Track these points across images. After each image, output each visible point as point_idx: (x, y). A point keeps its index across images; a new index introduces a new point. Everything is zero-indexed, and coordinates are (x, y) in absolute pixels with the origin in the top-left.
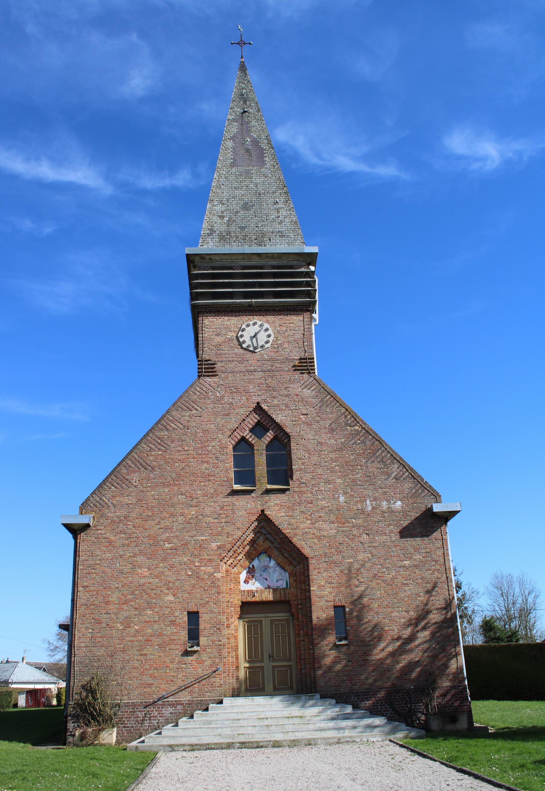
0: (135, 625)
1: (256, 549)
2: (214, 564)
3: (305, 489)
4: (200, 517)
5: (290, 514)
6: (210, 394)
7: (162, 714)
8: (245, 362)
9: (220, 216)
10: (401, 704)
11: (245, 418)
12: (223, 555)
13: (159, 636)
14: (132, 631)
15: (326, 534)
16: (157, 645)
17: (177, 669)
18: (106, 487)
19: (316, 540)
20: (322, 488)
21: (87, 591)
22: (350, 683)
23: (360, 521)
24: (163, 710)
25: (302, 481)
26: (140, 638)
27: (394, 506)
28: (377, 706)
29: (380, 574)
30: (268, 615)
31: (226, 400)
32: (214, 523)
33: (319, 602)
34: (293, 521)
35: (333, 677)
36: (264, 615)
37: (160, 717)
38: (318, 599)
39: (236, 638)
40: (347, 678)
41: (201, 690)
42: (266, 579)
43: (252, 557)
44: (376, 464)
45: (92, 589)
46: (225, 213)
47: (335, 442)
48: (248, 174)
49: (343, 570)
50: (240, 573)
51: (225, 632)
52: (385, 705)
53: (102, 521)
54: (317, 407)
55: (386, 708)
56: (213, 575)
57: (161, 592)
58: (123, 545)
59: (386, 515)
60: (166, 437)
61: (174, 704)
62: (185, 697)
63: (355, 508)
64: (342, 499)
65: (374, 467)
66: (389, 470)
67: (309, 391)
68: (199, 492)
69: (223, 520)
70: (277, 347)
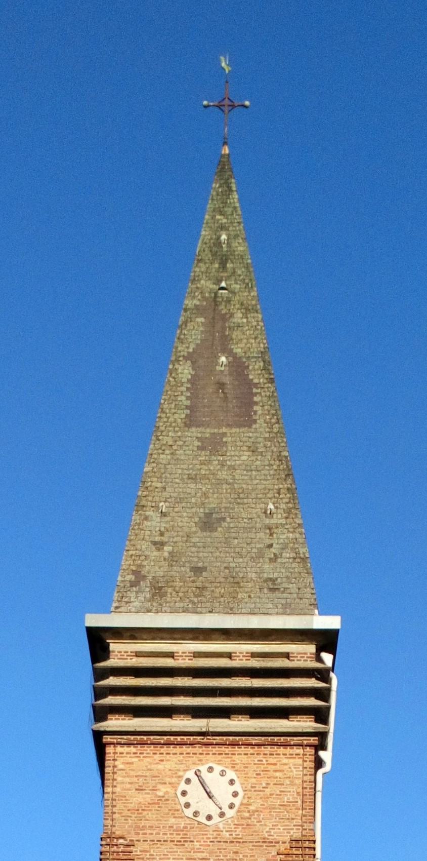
8: (186, 844)
9: (155, 543)
46: (167, 534)
48: (213, 445)
70: (246, 816)
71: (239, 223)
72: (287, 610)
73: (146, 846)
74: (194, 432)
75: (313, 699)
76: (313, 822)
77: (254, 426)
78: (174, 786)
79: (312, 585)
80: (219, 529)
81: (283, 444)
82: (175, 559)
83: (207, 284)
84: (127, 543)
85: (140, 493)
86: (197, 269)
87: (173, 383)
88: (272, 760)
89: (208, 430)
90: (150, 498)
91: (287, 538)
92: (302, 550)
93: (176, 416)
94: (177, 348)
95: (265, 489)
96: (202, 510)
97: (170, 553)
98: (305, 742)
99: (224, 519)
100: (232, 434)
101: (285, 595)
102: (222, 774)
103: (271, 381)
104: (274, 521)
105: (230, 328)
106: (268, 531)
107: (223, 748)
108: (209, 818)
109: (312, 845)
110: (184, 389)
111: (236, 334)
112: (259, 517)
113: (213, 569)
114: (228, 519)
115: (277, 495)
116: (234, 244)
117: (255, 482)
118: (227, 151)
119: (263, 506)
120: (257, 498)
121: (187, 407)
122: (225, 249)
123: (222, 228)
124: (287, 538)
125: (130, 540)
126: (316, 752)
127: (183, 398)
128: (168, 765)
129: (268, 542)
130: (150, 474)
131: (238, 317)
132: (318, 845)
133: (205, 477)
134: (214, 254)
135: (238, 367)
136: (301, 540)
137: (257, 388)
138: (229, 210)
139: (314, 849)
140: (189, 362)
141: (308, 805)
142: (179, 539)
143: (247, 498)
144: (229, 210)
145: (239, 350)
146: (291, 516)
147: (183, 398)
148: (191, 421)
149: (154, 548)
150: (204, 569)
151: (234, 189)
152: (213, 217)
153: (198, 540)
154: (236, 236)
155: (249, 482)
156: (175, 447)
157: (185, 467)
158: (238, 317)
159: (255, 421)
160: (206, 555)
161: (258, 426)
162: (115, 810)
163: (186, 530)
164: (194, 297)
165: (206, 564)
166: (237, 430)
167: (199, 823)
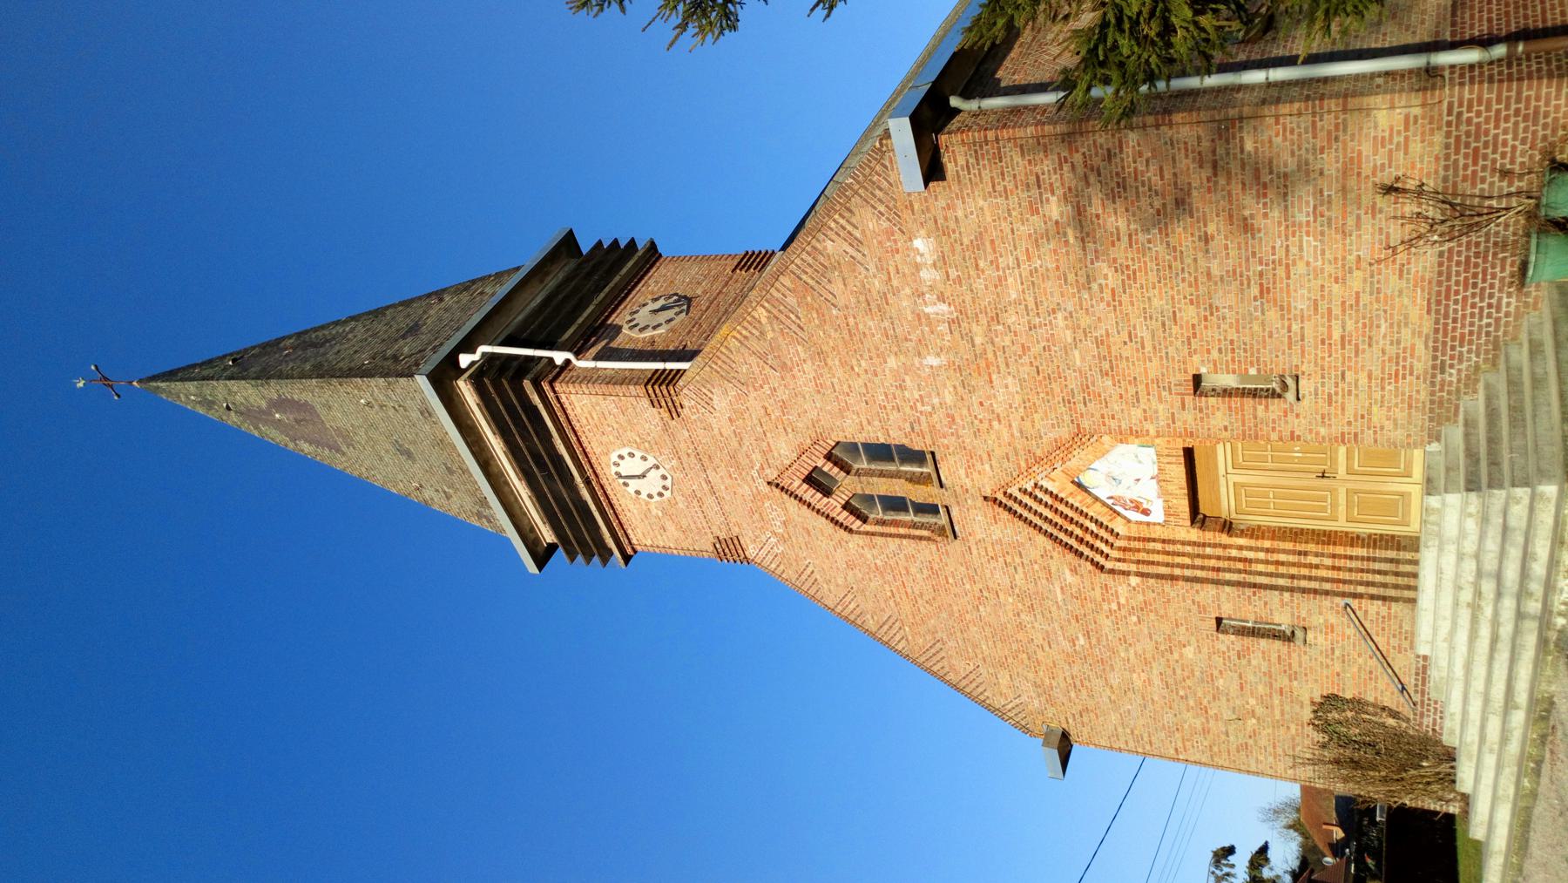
4: (1017, 591)
15: (1018, 399)
20: (917, 397)
25: (908, 429)
26: (1277, 702)
27: (927, 256)
28: (1480, 327)
29: (1107, 295)
30: (1222, 471)
33: (1185, 422)
34: (998, 452)
36: (1222, 481)
38: (1178, 424)
40: (1390, 383)
42: (1138, 480)
44: (837, 287)
47: (809, 362)
49: (1101, 371)
54: (744, 388)
55: (1490, 306)
56: (1134, 589)
60: (875, 618)
63: (948, 337)
64: (932, 360)
66: (842, 262)
67: (715, 397)
68: (968, 586)
69: (1018, 560)
88: (584, 421)
107: (593, 461)
108: (664, 478)
128: (631, 507)
162: (691, 548)
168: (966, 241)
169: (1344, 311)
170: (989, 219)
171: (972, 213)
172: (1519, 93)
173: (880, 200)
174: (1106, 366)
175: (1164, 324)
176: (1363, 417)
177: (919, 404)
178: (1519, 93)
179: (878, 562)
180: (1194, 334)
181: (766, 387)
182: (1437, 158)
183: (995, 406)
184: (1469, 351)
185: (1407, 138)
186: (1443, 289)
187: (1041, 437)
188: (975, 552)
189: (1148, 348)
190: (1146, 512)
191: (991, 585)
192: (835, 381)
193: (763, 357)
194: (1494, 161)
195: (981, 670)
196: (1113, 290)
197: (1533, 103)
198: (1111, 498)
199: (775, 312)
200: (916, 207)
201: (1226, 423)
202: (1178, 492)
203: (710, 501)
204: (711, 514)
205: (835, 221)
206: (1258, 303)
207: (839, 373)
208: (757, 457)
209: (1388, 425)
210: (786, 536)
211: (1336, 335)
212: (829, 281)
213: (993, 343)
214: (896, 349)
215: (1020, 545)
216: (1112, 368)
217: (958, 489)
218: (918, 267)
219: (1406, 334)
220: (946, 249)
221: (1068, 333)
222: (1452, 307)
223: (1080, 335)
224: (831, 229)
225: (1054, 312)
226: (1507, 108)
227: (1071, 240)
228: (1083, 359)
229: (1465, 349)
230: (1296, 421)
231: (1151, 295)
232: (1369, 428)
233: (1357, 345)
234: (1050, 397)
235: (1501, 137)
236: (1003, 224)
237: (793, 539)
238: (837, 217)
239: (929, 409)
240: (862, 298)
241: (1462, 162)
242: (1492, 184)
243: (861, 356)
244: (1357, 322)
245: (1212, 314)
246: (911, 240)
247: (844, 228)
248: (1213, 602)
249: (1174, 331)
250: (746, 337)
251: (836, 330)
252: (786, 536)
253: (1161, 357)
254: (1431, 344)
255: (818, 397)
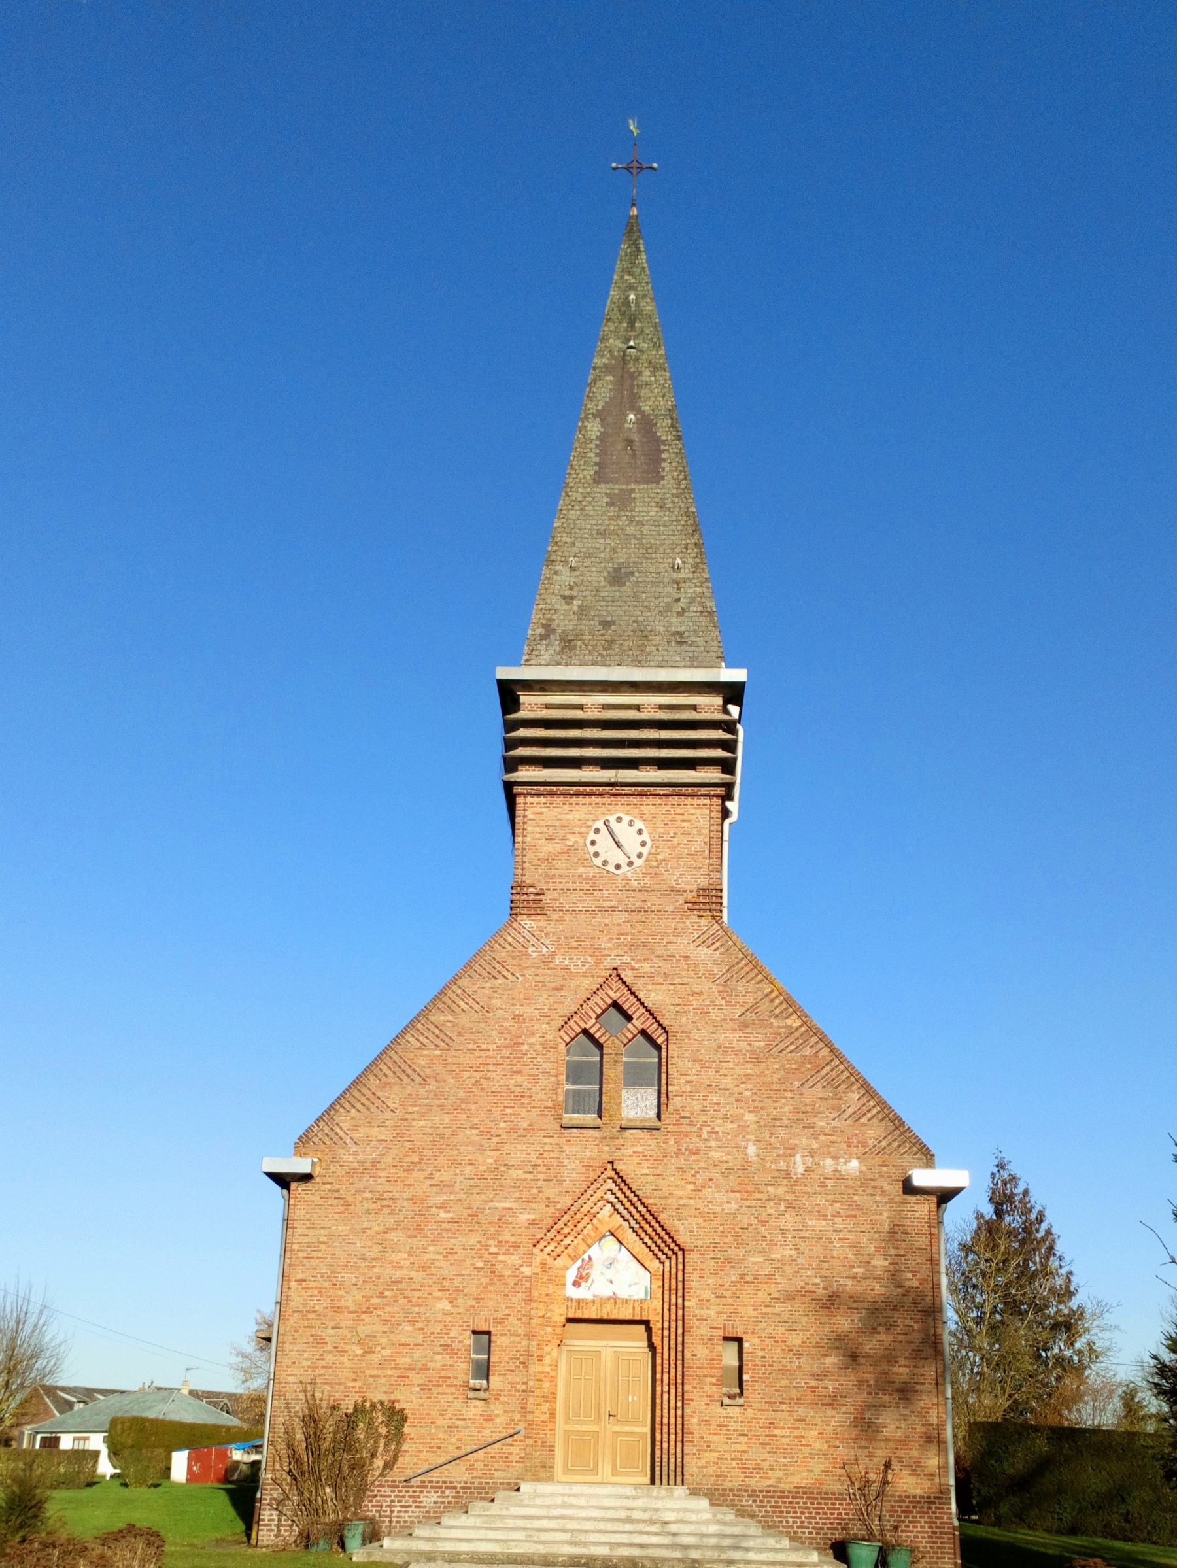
0: (382, 1348)
1: (597, 1229)
2: (521, 1251)
3: (689, 1129)
4: (502, 1168)
5: (658, 1172)
6: (531, 949)
7: (420, 1502)
8: (595, 893)
9: (564, 597)
10: (830, 1519)
11: (589, 996)
12: (539, 1236)
13: (421, 1369)
14: (375, 1358)
15: (718, 1209)
16: (418, 1385)
17: (448, 1427)
18: (341, 1110)
19: (700, 1220)
20: (717, 1129)
21: (303, 1288)
22: (742, 1473)
23: (781, 1191)
24: (422, 1495)
26: (390, 1372)
27: (844, 1167)
31: (557, 963)
32: (525, 1180)
33: (698, 1327)
34: (662, 1183)
35: (713, 1460)
37: (416, 1507)
38: (697, 1323)
39: (553, 1379)
41: (487, 1466)
42: (611, 1282)
43: (589, 1241)
44: (819, 1091)
45: (312, 1284)
46: (576, 589)
47: (748, 1048)
48: (622, 501)
50: (567, 1269)
51: (535, 1368)
52: (801, 1518)
53: (333, 1169)
55: (802, 1522)
57: (429, 1294)
58: (368, 1212)
59: (830, 1183)
60: (449, 1024)
61: (441, 1487)
62: (458, 1474)
64: (752, 1150)
65: (815, 1093)
66: (841, 1102)
67: (710, 951)
68: (502, 1125)
69: (541, 1176)
70: (654, 867)
71: (647, 283)
72: (695, 663)
73: (555, 895)
74: (603, 488)
75: (719, 750)
76: (720, 871)
77: (662, 482)
78: (583, 835)
79: (719, 639)
80: (628, 584)
81: (690, 500)
82: (584, 613)
83: (615, 343)
84: (537, 597)
85: (549, 548)
86: (606, 329)
87: (582, 440)
89: (617, 486)
90: (560, 553)
91: (695, 592)
92: (709, 605)
93: (586, 472)
94: (586, 405)
95: (672, 544)
96: (610, 565)
97: (579, 607)
98: (712, 793)
99: (632, 574)
100: (640, 490)
101: (692, 648)
102: (631, 823)
103: (679, 438)
104: (681, 576)
105: (638, 386)
106: (675, 586)
107: (632, 798)
108: (618, 867)
109: (719, 894)
110: (593, 446)
111: (644, 392)
112: (666, 571)
113: (622, 623)
114: (636, 574)
115: (684, 550)
116: (643, 304)
117: (663, 537)
118: (635, 213)
119: (670, 560)
120: (664, 553)
121: (596, 464)
122: (633, 309)
123: (631, 287)
124: (695, 592)
125: (540, 595)
126: (723, 803)
127: (592, 455)
129: (676, 596)
130: (560, 530)
131: (646, 375)
132: (725, 894)
133: (614, 532)
134: (623, 314)
135: (647, 424)
136: (708, 595)
137: (665, 445)
138: (637, 271)
139: (721, 897)
140: (598, 419)
141: (715, 854)
142: (588, 593)
143: (655, 553)
144: (637, 271)
145: (647, 408)
146: (698, 570)
147: (592, 455)
148: (600, 477)
149: (563, 602)
150: (613, 623)
151: (642, 249)
152: (622, 277)
153: (606, 594)
154: (644, 296)
155: (657, 537)
156: (584, 503)
157: (595, 522)
158: (646, 375)
159: (663, 478)
160: (614, 608)
161: (665, 482)
162: (525, 859)
163: (595, 584)
164: (603, 356)
165: (614, 618)
166: (646, 486)
167: (608, 872)
168: (856, 1198)
169: (797, 1437)
170: (873, 1217)
171: (878, 1206)
172: (946, 1533)
173: (890, 1144)
174: (749, 1279)
175: (786, 1322)
176: (708, 1446)
177: (709, 1129)
178: (946, 1533)
179: (525, 1048)
180: (778, 1342)
181: (723, 1002)
182: (905, 1491)
183: (710, 1190)
184: (767, 1511)
185: (920, 1475)
186: (815, 1495)
187: (680, 1220)
188: (547, 1140)
189: (765, 1310)
190: (576, 1284)
191: (507, 1147)
192: (731, 1065)
193: (752, 1008)
194: (904, 1522)
195: (388, 1114)
196: (815, 1292)
197: (939, 1541)
198: (590, 1258)
199: (797, 1034)
200: (884, 1169)
201: (699, 1356)
202: (605, 1311)
203: (590, 902)
204: (574, 897)
205: (874, 1107)
206: (803, 1385)
207: (739, 1071)
208: (646, 968)
209: (702, 1463)
210: (551, 965)
211: (776, 1432)
212: (824, 1087)
213: (769, 1200)
214: (762, 1123)
215: (560, 1182)
216: (747, 1282)
217: (620, 1141)
218: (835, 1158)
219: (780, 1474)
220: (850, 1183)
221: (779, 1256)
222: (801, 1501)
223: (776, 1264)
224: (868, 1101)
225: (796, 1249)
226: (937, 1527)
227: (855, 1270)
228: (755, 1263)
229: (768, 1509)
230: (703, 1403)
231: (810, 1317)
232: (698, 1450)
233: (770, 1444)
234: (719, 1233)
235: (919, 1525)
236: (868, 1226)
237: (546, 971)
238: (879, 1108)
239: (705, 1136)
240: (809, 1109)
241: (904, 1505)
242: (889, 1521)
243: (756, 1093)
244: (788, 1445)
245: (794, 1355)
246: (857, 1158)
247: (869, 1111)
248: (509, 1331)
249: (780, 1328)
250: (772, 1001)
251: (780, 1079)
252: (551, 965)
253: (757, 1317)
254: (771, 1489)
255: (714, 1045)
